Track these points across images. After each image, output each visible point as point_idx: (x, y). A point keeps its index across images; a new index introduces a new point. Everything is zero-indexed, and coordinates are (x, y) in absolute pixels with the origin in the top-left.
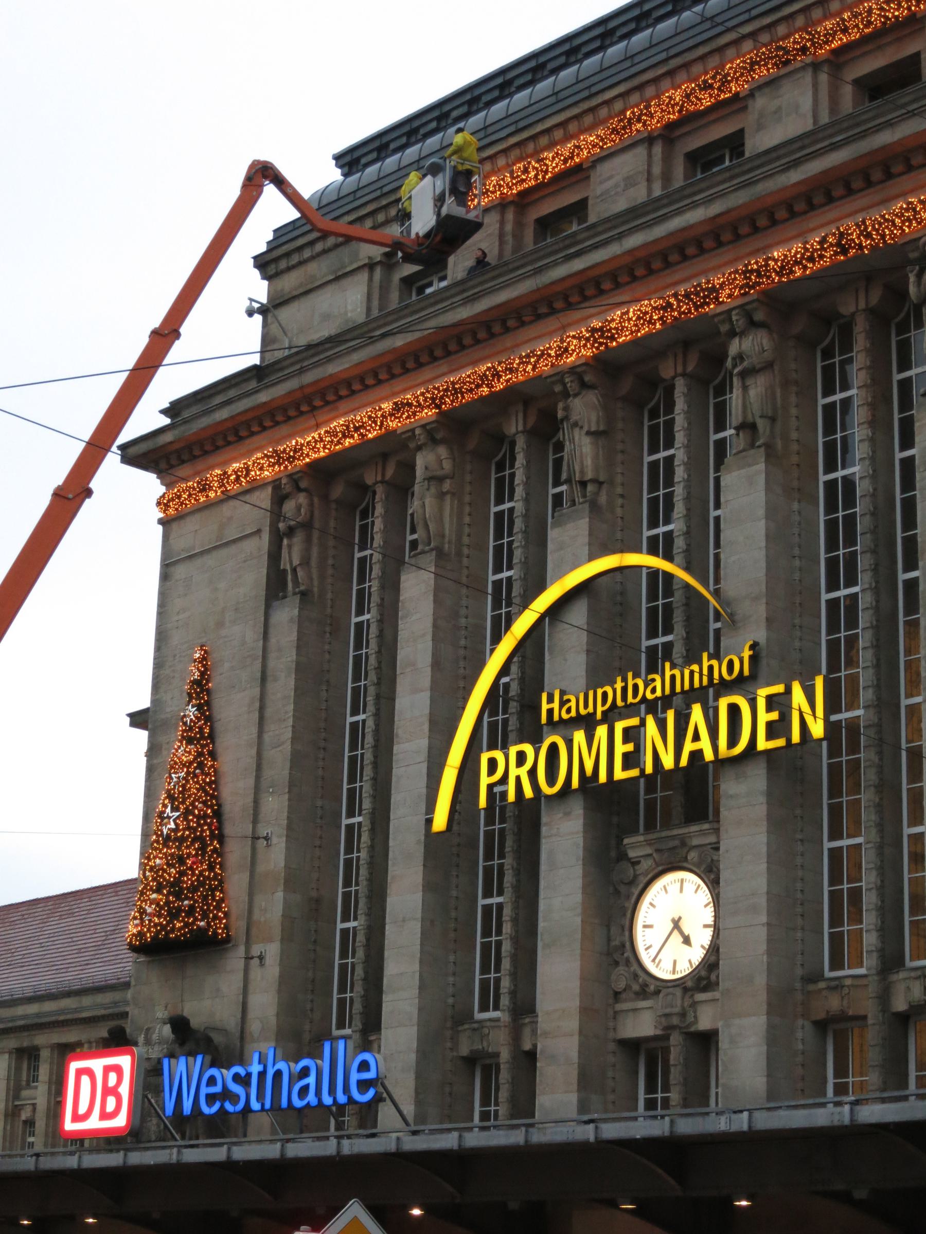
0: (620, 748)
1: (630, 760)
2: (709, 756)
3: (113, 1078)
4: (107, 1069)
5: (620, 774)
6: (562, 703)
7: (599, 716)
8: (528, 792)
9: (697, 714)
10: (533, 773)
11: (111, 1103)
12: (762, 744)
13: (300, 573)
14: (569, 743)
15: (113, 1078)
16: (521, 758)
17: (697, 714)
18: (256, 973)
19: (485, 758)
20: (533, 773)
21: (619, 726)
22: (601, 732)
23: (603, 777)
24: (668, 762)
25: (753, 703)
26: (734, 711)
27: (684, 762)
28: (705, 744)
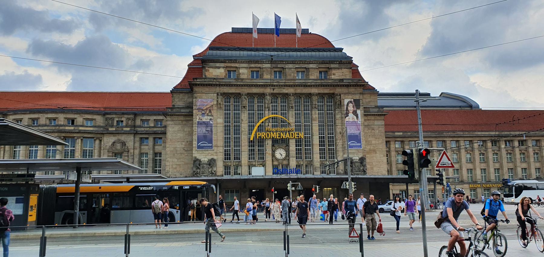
1: (279, 137)
2: (289, 138)
5: (277, 138)
6: (269, 129)
7: (274, 131)
8: (265, 138)
9: (288, 133)
10: (265, 136)
12: (296, 138)
14: (270, 133)
16: (263, 134)
17: (288, 133)
19: (258, 133)
20: (265, 136)
21: (277, 133)
22: (275, 133)
23: (275, 138)
24: (284, 137)
25: (294, 133)
26: (292, 134)
27: (286, 138)
28: (289, 136)
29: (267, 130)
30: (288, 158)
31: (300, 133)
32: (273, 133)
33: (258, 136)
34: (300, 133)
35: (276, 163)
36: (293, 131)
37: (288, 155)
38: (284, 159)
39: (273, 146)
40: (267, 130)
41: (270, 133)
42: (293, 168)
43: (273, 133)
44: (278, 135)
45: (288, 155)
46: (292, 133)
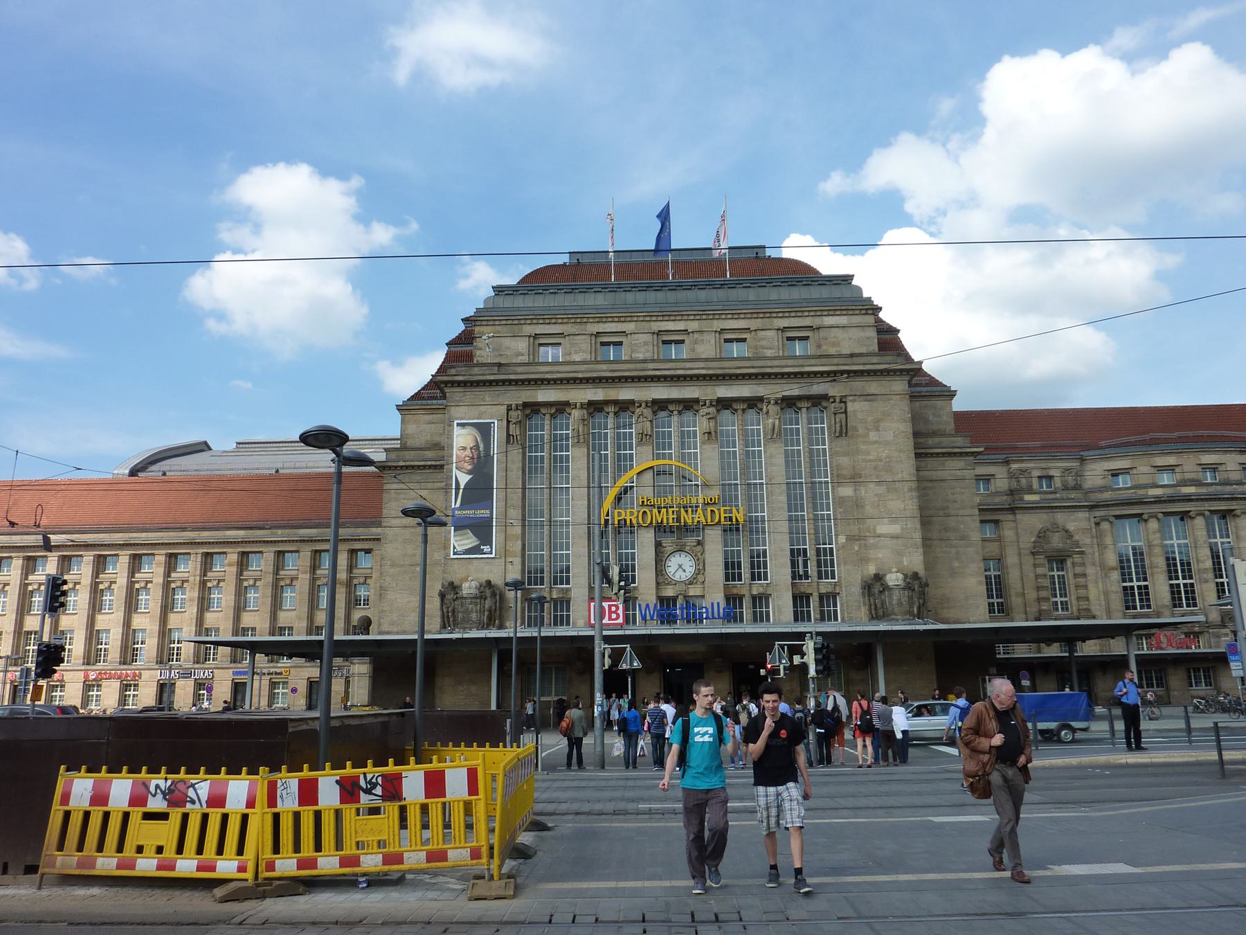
0: (671, 516)
3: (613, 609)
4: (610, 607)
11: (614, 616)
12: (722, 520)
13: (518, 437)
14: (651, 511)
15: (613, 609)
16: (632, 513)
18: (509, 567)
22: (664, 510)
24: (689, 522)
29: (643, 502)
30: (700, 578)
31: (734, 509)
32: (659, 512)
33: (616, 519)
34: (734, 509)
35: (669, 592)
36: (715, 503)
37: (700, 570)
38: (691, 582)
39: (658, 545)
40: (643, 502)
41: (651, 511)
42: (712, 604)
43: (659, 512)
44: (671, 516)
45: (700, 570)
46: (712, 511)
